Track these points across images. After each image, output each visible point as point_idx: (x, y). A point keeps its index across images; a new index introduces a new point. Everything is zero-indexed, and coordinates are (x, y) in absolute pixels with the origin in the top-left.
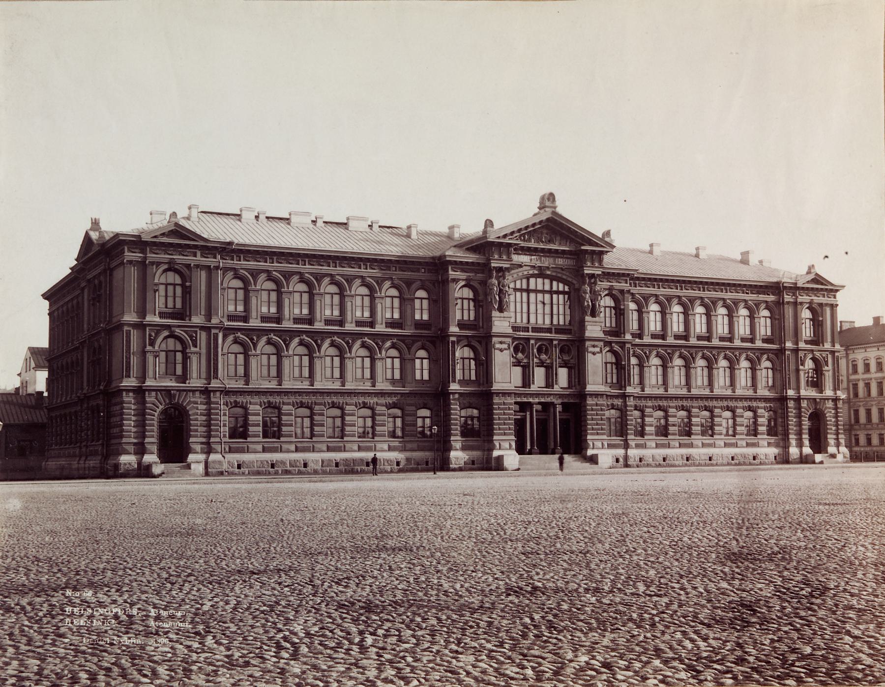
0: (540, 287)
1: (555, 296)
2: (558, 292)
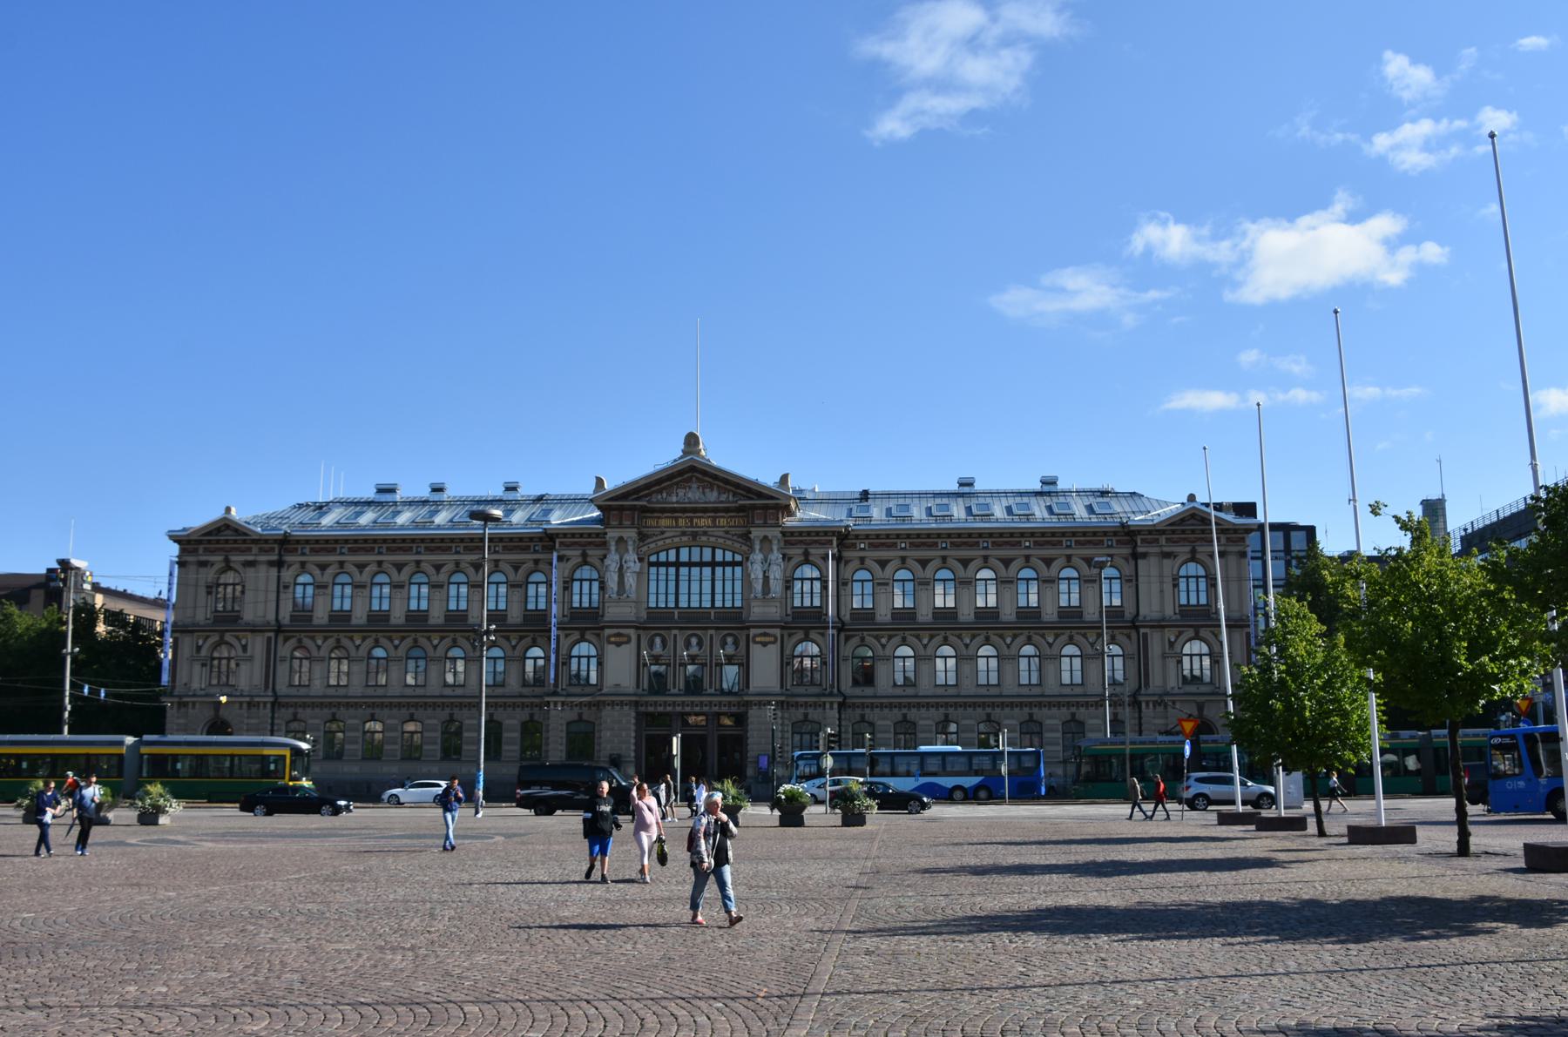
0: (696, 558)
1: (719, 570)
2: (724, 564)
